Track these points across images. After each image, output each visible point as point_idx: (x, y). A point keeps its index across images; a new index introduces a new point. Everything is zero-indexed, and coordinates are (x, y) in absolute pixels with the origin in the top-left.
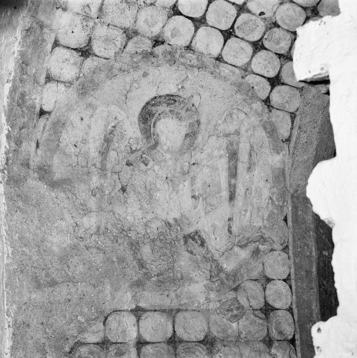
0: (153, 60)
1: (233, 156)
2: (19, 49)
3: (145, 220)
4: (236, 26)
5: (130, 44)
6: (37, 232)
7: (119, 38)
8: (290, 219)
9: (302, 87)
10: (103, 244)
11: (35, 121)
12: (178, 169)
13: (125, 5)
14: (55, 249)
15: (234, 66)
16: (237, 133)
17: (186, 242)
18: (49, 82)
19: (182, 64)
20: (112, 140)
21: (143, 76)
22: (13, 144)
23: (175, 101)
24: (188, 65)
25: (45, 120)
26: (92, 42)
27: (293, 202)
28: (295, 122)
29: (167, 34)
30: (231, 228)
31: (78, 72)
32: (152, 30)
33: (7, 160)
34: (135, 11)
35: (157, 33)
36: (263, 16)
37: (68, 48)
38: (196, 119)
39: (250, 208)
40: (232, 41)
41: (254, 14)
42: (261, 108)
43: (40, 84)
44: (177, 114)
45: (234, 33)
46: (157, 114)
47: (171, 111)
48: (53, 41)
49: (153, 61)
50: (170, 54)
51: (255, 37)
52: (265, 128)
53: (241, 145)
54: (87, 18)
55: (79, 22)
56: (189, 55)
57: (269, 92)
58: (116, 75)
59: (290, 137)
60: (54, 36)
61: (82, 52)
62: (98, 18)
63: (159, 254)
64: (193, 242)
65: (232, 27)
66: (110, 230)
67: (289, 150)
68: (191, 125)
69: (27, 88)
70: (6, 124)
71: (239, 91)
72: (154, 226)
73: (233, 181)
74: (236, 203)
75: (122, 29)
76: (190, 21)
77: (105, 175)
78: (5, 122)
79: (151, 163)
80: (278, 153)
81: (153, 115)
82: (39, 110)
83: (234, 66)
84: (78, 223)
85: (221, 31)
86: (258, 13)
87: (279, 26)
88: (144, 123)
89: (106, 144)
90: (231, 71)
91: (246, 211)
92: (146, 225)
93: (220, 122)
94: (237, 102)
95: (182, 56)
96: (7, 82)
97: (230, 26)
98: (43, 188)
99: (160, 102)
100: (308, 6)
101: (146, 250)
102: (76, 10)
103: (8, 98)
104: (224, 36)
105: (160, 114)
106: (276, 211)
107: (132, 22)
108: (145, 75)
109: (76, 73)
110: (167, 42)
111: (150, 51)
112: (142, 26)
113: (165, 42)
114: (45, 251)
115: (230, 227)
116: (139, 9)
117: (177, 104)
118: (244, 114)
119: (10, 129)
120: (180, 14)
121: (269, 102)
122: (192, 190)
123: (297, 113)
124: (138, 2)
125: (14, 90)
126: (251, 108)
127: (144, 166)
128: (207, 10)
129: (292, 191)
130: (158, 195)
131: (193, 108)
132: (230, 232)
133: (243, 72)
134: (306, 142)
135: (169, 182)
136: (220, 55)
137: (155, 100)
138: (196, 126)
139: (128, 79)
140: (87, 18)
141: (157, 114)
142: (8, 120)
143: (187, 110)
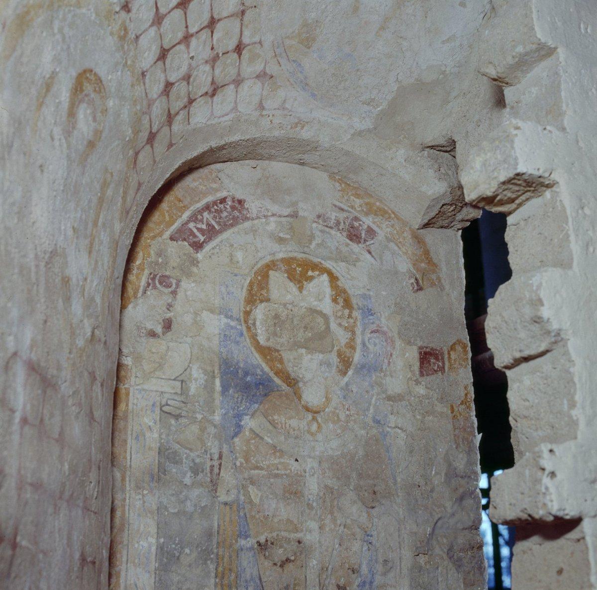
41: (189, 53)
87: (188, 83)
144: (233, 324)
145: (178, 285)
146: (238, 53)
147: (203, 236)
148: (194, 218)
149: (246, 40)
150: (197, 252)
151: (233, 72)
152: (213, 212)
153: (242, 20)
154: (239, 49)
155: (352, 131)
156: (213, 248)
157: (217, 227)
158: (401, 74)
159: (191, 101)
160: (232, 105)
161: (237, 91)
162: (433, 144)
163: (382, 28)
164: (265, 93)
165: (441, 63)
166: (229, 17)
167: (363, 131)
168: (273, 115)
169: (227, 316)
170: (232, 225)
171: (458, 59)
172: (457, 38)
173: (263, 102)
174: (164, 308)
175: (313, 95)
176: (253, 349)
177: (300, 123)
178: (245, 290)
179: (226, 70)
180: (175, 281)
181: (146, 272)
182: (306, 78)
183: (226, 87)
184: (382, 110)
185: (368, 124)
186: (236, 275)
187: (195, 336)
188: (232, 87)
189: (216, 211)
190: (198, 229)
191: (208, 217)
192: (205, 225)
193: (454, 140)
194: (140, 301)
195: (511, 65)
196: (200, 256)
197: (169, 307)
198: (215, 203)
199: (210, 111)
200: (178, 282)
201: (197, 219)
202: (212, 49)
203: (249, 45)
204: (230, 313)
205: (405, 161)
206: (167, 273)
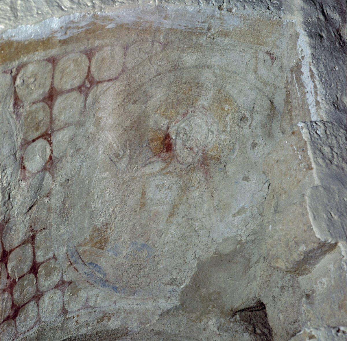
146: (33, 273)
149: (40, 259)
151: (30, 291)
154: (34, 269)
155: (159, 312)
158: (198, 251)
161: (38, 305)
162: (243, 308)
163: (172, 215)
164: (66, 299)
165: (235, 234)
166: (20, 245)
167: (171, 309)
168: (78, 316)
171: (252, 228)
172: (247, 209)
173: (66, 308)
175: (115, 289)
177: (106, 316)
182: (105, 275)
184: (186, 287)
185: (174, 302)
188: (33, 303)
193: (262, 303)
195: (298, 261)
199: (14, 331)
202: (8, 277)
203: (43, 262)
205: (218, 329)
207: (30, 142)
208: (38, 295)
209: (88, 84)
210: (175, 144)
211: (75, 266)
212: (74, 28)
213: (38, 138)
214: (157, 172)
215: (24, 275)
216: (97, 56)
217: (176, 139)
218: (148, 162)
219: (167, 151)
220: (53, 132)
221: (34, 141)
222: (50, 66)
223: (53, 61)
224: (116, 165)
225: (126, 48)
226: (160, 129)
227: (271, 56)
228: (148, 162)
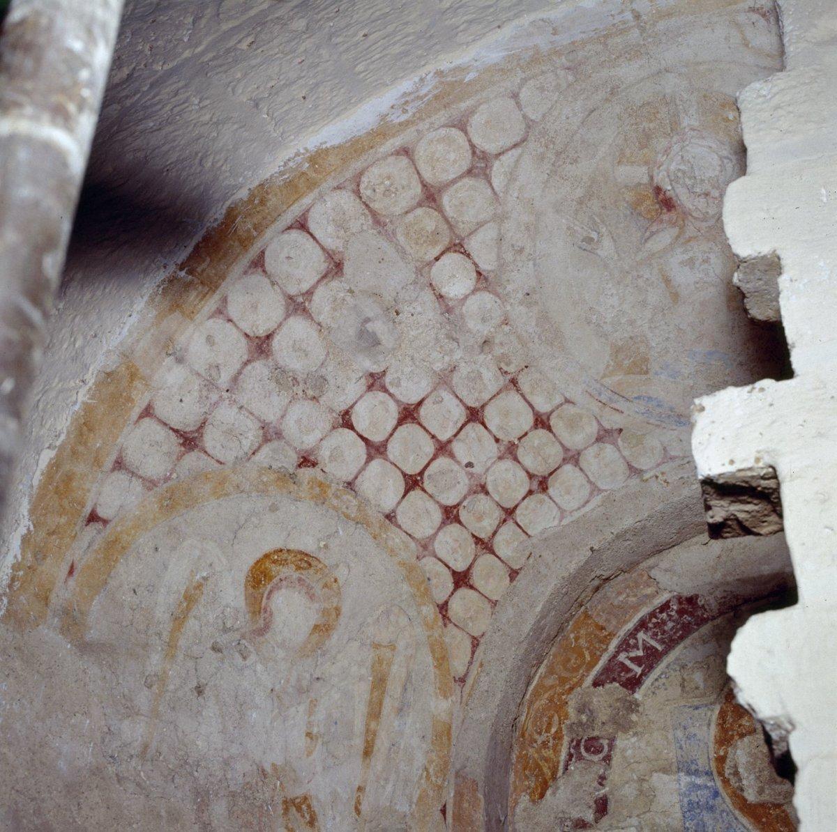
0: (292, 487)
1: (380, 683)
2: (85, 399)
3: (226, 755)
4: (426, 474)
5: (266, 449)
6: (36, 725)
7: (250, 435)
8: (451, 812)
9: (497, 601)
10: (148, 778)
11: (77, 528)
12: (293, 680)
13: (273, 385)
14: (61, 764)
15: (410, 535)
16: (392, 647)
17: (286, 810)
18: (119, 470)
19: (335, 508)
20: (197, 600)
21: (270, 510)
22: (29, 556)
23: (310, 565)
24: (343, 513)
25: (95, 531)
26: (206, 428)
27: (457, 785)
28: (476, 654)
29: (324, 454)
30: (360, 804)
31: (169, 468)
32: (304, 439)
33: (13, 579)
34: (287, 401)
35: (310, 446)
36: (468, 469)
37: (165, 424)
38: (335, 605)
39: (393, 777)
40: (415, 494)
41: (458, 463)
42: (432, 616)
43: (104, 469)
44: (308, 587)
45: (422, 483)
46: (278, 577)
47: (300, 580)
48: (144, 406)
49: (291, 490)
50: (320, 486)
51: (450, 500)
52: (433, 651)
53: (394, 668)
54: (210, 384)
55: (196, 387)
56: (348, 497)
57: (449, 593)
58: (227, 495)
59: (466, 675)
60: (149, 398)
61: (186, 439)
62: (227, 391)
63: (240, 821)
64: (298, 815)
65: (421, 473)
66: (164, 757)
67: (462, 697)
68: (325, 612)
69: (80, 468)
70: (27, 518)
71: (409, 580)
72: (241, 767)
73: (373, 725)
74: (373, 764)
75: (260, 421)
76: (363, 443)
77: (173, 657)
78: (26, 513)
79: (253, 657)
80: (446, 697)
81: (271, 579)
82: (89, 512)
83: (410, 535)
84: (112, 729)
85: (404, 475)
86: (465, 462)
87: (487, 493)
88: (254, 587)
89: (185, 605)
90: (403, 542)
91: (387, 780)
92: (226, 763)
93: (369, 620)
94: (400, 595)
95: (337, 497)
96: (49, 448)
97: (418, 471)
98: (65, 647)
99: (286, 560)
100: (536, 473)
101: (219, 809)
102: (196, 367)
103: (42, 474)
104: (407, 484)
105: (281, 580)
106: (431, 793)
107: (279, 414)
108: (274, 508)
109: (166, 470)
110: (320, 466)
111: (291, 471)
112: (290, 427)
113: (317, 464)
114: (42, 763)
115: (358, 802)
116: (294, 399)
117: (312, 571)
118: (406, 619)
119: (32, 528)
120: (352, 427)
121: (446, 611)
122: (309, 722)
123: (482, 641)
124: (295, 388)
125: (55, 465)
126: (419, 613)
127: (240, 659)
128: (391, 435)
129: (458, 766)
130: (254, 715)
131: (335, 586)
132: (358, 811)
133: (421, 549)
134: (487, 691)
135: (275, 699)
136: (394, 511)
137: (280, 554)
138: (334, 616)
139: (246, 507)
140: (210, 384)
141: (278, 577)
142: (32, 512)
143: (326, 586)
144: (699, 781)
145: (611, 747)
146: (543, 427)
147: (640, 666)
148: (625, 646)
149: (543, 407)
150: (634, 692)
152: (651, 628)
153: (518, 391)
154: (541, 422)
156: (656, 680)
157: (660, 648)
159: (510, 512)
160: (588, 486)
168: (663, 473)
169: (689, 773)
170: (682, 638)
174: (595, 784)
176: (737, 812)
178: (713, 727)
179: (540, 452)
180: (607, 741)
181: (566, 740)
183: (558, 471)
186: (697, 708)
187: (644, 813)
189: (656, 625)
190: (632, 659)
191: (645, 637)
192: (641, 651)
194: (561, 782)
196: (638, 696)
197: (602, 779)
198: (653, 614)
200: (612, 741)
201: (628, 645)
202: (497, 440)
203: (552, 412)
204: (693, 767)
206: (596, 733)
207: (430, 262)
208: (573, 457)
209: (480, 165)
210: (677, 196)
211: (612, 405)
212: (413, 101)
213: (443, 253)
214: (671, 244)
215: (526, 434)
216: (477, 121)
217: (673, 188)
218: (648, 234)
219: (669, 210)
220: (463, 239)
221: (437, 259)
222: (404, 161)
223: (406, 152)
224: (597, 254)
225: (515, 96)
226: (639, 184)
227: (760, 14)
228: (648, 234)
